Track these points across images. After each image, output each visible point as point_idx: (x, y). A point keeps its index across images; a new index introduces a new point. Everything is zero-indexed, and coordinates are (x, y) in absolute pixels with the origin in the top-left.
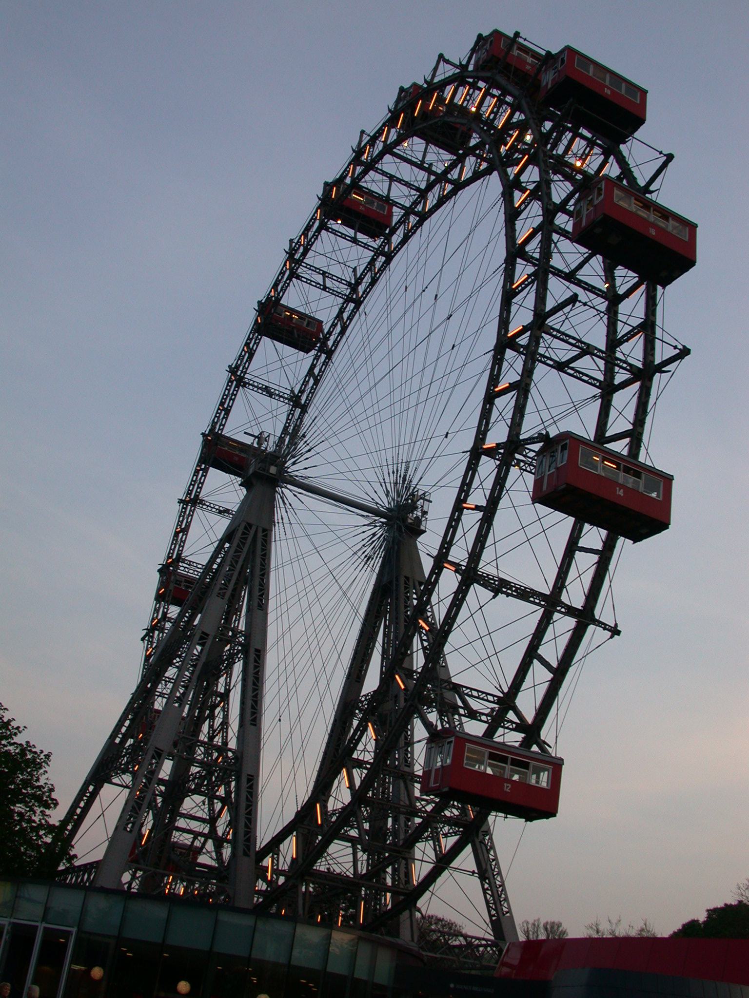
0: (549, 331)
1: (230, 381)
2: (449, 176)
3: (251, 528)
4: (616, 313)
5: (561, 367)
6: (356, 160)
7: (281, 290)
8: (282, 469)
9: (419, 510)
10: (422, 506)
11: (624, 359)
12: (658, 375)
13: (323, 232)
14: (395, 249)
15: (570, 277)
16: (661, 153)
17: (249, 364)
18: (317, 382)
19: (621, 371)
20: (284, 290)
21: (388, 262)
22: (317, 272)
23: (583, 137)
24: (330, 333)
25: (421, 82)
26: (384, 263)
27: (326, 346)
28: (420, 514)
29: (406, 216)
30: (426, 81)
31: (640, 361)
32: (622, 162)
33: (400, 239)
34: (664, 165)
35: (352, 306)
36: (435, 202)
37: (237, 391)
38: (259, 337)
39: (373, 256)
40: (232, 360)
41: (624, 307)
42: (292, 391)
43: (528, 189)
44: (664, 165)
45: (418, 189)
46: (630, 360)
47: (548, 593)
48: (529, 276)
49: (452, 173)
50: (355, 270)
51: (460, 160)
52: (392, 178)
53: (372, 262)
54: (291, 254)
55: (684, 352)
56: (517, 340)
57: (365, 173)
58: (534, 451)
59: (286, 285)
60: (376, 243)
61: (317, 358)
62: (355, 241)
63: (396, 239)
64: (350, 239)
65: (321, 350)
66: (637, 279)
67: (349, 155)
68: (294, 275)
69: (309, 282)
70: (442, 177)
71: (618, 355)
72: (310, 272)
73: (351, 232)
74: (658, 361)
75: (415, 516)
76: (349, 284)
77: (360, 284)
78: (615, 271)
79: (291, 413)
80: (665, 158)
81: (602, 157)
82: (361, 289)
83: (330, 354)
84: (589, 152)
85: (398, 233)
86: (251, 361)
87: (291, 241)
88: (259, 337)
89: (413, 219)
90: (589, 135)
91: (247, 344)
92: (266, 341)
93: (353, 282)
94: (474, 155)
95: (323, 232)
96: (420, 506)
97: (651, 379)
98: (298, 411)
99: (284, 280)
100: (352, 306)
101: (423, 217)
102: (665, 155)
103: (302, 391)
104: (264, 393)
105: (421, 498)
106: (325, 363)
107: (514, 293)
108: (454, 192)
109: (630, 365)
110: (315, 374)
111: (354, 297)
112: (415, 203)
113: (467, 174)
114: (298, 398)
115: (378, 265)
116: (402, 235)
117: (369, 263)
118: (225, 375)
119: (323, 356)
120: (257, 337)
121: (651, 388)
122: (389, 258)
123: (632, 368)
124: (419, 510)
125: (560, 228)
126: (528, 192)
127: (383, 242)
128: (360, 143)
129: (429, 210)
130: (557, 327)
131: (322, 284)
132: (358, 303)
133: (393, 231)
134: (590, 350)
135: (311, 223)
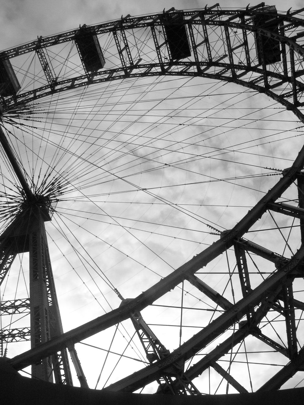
6: (202, 13)
7: (101, 31)
13: (149, 27)
18: (72, 87)
20: (103, 32)
21: (160, 74)
24: (100, 74)
26: (158, 72)
27: (93, 78)
29: (191, 64)
33: (177, 71)
35: (123, 73)
39: (156, 64)
40: (45, 35)
42: (57, 78)
45: (211, 60)
50: (140, 60)
52: (206, 40)
54: (123, 20)
59: (106, 31)
63: (174, 68)
68: (114, 30)
76: (132, 64)
77: (136, 68)
79: (46, 87)
82: (135, 71)
83: (91, 82)
85: (179, 66)
86: (52, 45)
87: (129, 16)
89: (193, 69)
91: (60, 36)
95: (149, 27)
99: (107, 28)
100: (123, 73)
101: (200, 73)
104: (43, 66)
108: (229, 80)
111: (128, 71)
112: (202, 63)
114: (56, 84)
115: (154, 70)
118: (34, 38)
122: (164, 72)
129: (206, 74)
132: (127, 75)
133: (177, 64)
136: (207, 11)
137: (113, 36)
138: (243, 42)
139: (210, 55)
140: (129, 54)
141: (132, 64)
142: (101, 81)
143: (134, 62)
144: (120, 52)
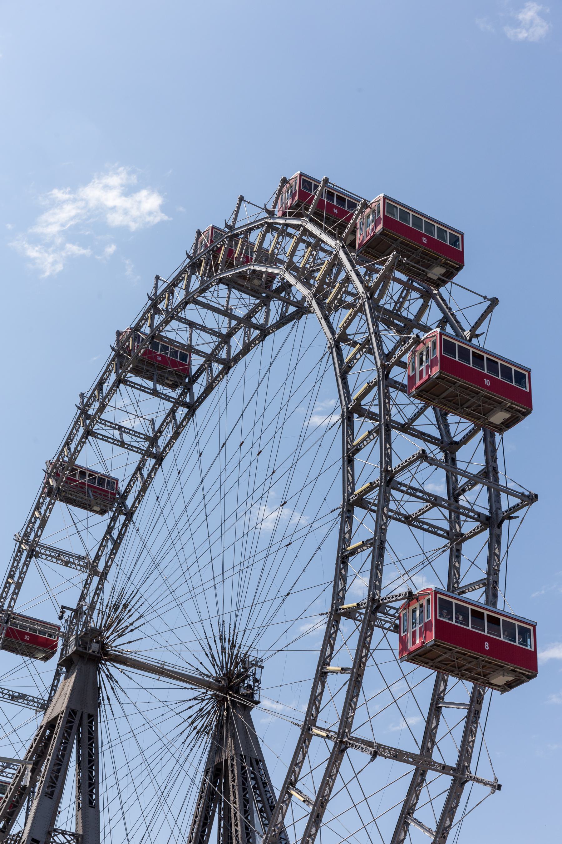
0: (398, 486)
1: (20, 551)
2: (253, 320)
3: (75, 715)
4: (454, 460)
5: (408, 520)
6: (154, 308)
8: (103, 646)
9: (251, 678)
10: (254, 674)
11: (470, 507)
12: (506, 522)
13: (122, 386)
14: (198, 399)
15: (406, 428)
16: (485, 298)
17: (42, 532)
18: (116, 545)
19: (468, 519)
22: (113, 427)
23: (399, 281)
24: (127, 491)
25: (222, 226)
27: (126, 507)
28: (251, 683)
30: (227, 226)
31: (487, 509)
32: (444, 306)
34: (489, 310)
36: (241, 347)
37: (29, 562)
38: (53, 501)
41: (462, 454)
43: (357, 343)
44: (489, 310)
46: (476, 508)
47: (418, 752)
48: (370, 433)
49: (257, 316)
51: (265, 302)
53: (173, 412)
55: (532, 499)
56: (364, 497)
57: (166, 322)
58: (394, 608)
60: (174, 394)
61: (114, 519)
62: (154, 393)
63: (198, 389)
64: (149, 391)
65: (119, 512)
66: (473, 425)
67: (143, 303)
68: (89, 433)
69: (105, 439)
70: (246, 321)
71: (461, 503)
72: (106, 428)
73: (150, 384)
74: (504, 507)
75: (246, 685)
76: (147, 438)
78: (447, 418)
80: (489, 303)
81: (421, 301)
83: (130, 515)
84: (407, 295)
85: (200, 380)
88: (53, 501)
90: (404, 278)
92: (60, 506)
93: (151, 434)
94: (280, 299)
95: (122, 386)
96: (252, 674)
97: (500, 526)
98: (96, 579)
101: (228, 365)
102: (489, 300)
103: (97, 558)
105: (253, 665)
106: (125, 525)
107: (357, 449)
109: (479, 514)
110: (113, 539)
113: (273, 319)
116: (205, 384)
117: (168, 415)
119: (122, 518)
120: (50, 501)
121: (501, 534)
122: (192, 408)
123: (479, 517)
124: (251, 678)
125: (396, 382)
126: (358, 345)
127: (183, 391)
128: (156, 289)
130: (407, 482)
131: (120, 440)
132: (159, 459)
133: (194, 379)
134: (438, 502)
135: (105, 376)
136: (155, 302)
137: (94, 438)
138: (227, 287)
139: (212, 332)
140: (129, 431)
141: (147, 438)
142: (139, 499)
143: (148, 434)
144: (122, 444)
